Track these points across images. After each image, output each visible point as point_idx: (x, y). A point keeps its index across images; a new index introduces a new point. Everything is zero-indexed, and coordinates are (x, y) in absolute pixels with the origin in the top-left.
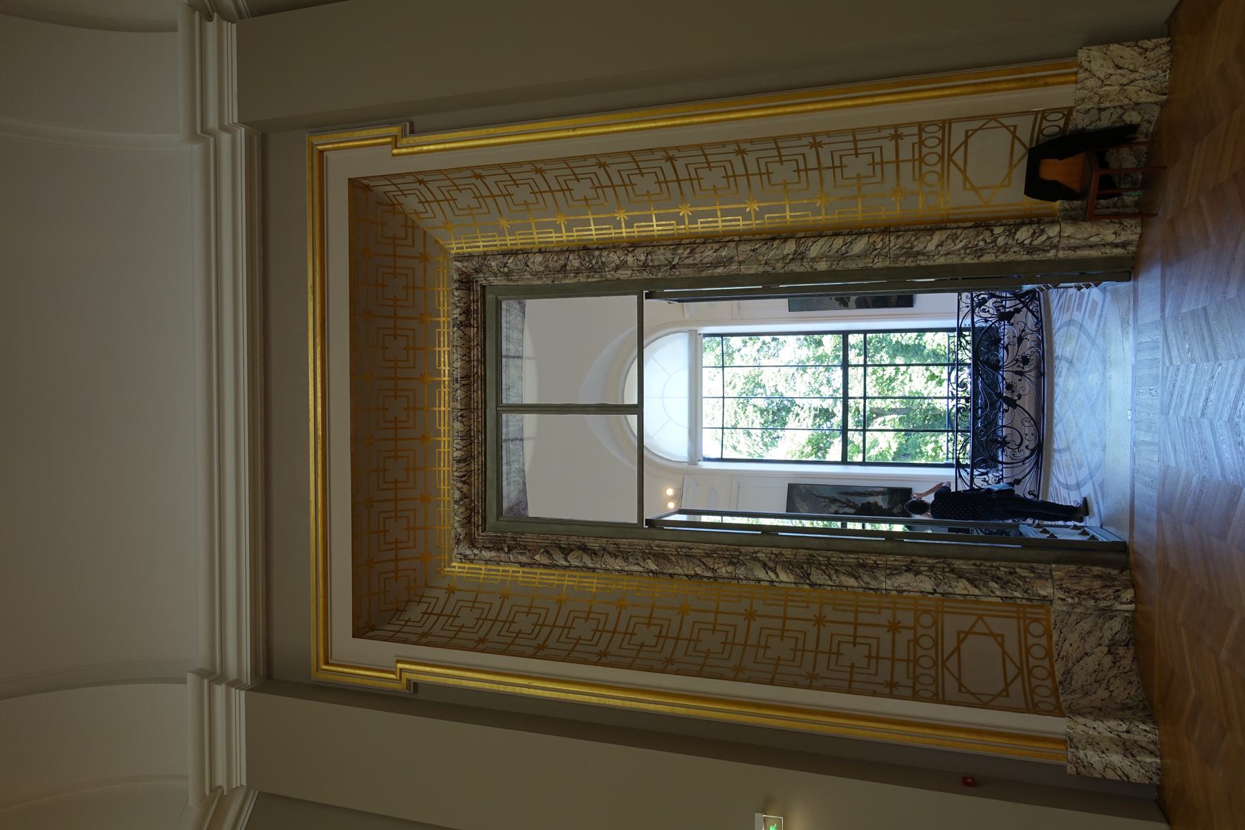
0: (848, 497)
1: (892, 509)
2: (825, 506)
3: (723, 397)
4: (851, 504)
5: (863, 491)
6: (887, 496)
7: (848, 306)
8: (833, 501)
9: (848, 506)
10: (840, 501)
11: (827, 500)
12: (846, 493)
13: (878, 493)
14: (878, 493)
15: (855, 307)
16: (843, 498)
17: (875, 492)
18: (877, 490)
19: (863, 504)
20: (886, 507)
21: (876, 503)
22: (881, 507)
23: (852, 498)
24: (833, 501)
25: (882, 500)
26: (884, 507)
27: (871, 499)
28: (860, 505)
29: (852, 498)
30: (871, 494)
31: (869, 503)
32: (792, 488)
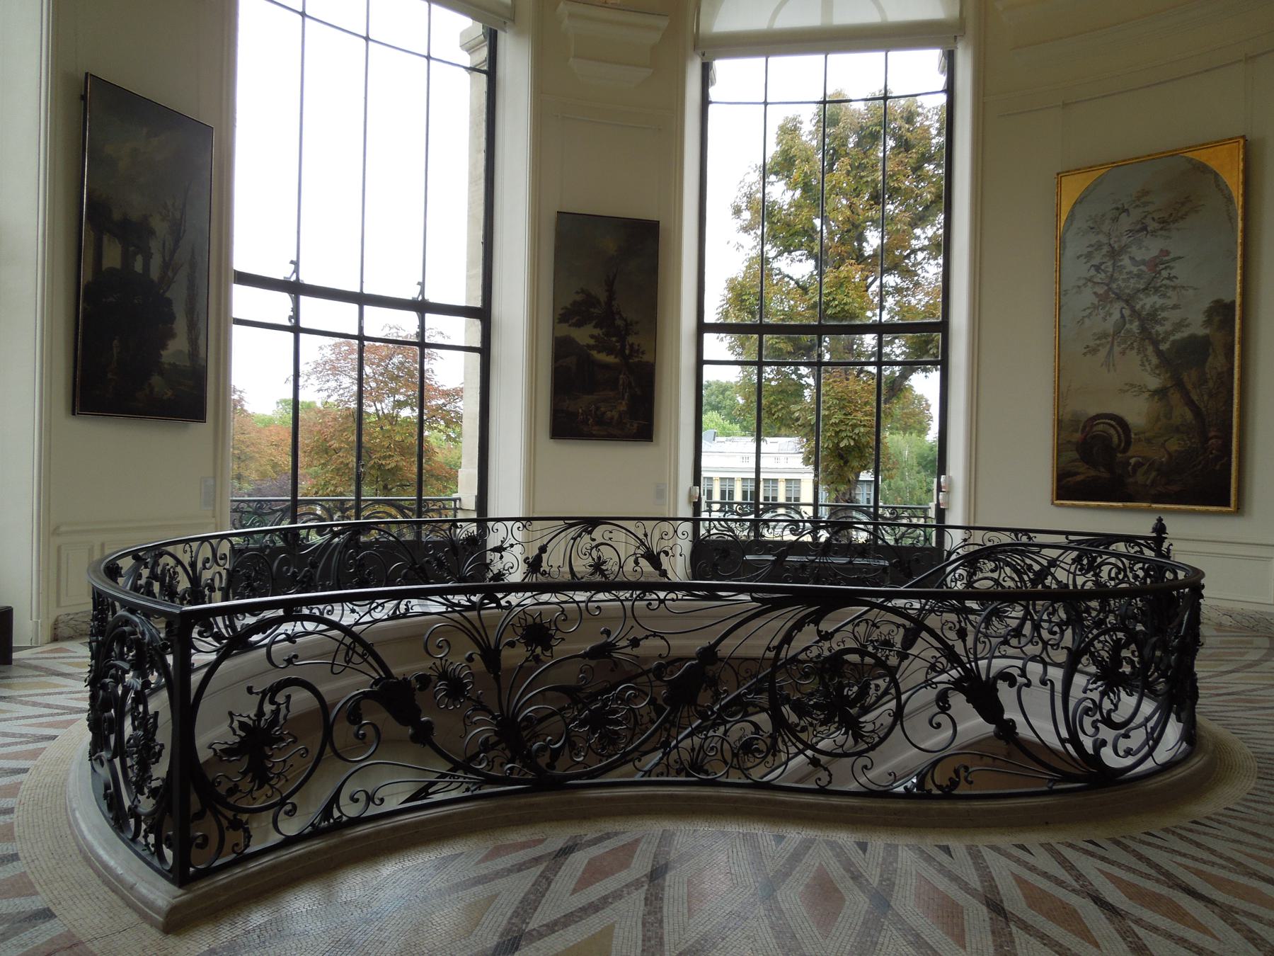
3: (766, 103)
9: (166, 266)
14: (194, 342)
15: (558, 334)
19: (169, 302)
20: (163, 360)
21: (171, 335)
22: (164, 346)
26: (164, 353)
27: (180, 325)
28: (168, 295)
30: (192, 326)
31: (171, 318)
32: (655, 225)
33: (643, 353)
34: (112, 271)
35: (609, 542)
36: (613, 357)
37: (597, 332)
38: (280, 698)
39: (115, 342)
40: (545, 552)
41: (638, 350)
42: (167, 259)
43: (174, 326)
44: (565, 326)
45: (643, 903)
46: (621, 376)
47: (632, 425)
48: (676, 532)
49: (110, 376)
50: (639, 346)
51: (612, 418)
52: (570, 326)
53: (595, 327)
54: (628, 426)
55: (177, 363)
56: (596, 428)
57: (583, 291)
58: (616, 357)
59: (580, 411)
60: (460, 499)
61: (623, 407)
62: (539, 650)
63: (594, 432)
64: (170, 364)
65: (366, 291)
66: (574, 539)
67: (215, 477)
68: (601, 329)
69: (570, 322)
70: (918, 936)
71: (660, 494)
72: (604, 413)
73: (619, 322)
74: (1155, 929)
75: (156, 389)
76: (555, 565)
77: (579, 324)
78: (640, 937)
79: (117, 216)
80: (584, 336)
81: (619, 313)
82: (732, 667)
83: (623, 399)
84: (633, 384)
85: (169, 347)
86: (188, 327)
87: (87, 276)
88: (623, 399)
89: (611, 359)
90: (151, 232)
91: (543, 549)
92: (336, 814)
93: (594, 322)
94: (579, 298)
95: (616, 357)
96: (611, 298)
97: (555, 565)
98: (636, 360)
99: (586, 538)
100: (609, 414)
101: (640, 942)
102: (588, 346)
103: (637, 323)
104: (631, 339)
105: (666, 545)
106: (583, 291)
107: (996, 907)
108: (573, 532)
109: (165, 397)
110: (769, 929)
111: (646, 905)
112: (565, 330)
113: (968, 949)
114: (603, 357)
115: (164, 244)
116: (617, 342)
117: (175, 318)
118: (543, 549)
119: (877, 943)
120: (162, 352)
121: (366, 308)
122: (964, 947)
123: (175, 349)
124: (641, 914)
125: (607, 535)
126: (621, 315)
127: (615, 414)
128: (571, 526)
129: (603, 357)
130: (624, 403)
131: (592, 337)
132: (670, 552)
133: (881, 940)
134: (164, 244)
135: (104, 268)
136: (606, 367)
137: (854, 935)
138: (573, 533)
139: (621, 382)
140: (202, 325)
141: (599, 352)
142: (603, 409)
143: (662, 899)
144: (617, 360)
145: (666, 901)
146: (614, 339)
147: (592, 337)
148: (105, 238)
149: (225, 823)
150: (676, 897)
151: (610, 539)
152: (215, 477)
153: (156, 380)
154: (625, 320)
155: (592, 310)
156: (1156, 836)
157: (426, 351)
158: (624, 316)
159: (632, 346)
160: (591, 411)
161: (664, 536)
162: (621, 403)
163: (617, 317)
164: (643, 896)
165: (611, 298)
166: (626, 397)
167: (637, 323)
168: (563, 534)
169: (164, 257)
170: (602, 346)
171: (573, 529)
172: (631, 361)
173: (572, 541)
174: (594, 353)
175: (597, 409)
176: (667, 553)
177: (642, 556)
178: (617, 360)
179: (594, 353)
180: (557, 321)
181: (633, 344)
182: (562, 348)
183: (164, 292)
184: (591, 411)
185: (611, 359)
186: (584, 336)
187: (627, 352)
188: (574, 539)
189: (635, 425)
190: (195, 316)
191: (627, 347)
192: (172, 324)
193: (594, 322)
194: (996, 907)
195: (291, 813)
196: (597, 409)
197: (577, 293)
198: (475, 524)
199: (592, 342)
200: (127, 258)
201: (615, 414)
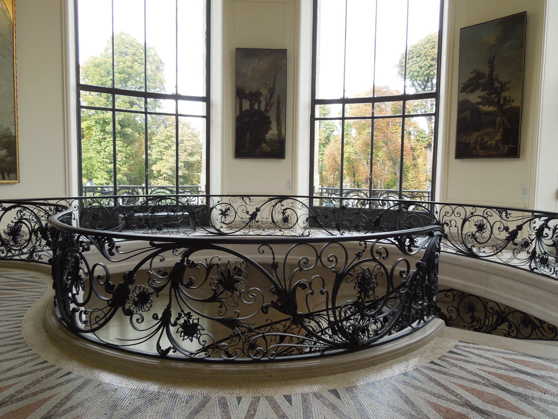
0: (276, 104)
1: (266, 143)
2: (266, 84)
4: (269, 107)
5: (281, 117)
6: (277, 138)
7: (461, 93)
8: (272, 92)
9: (267, 105)
10: (271, 97)
11: (272, 86)
12: (279, 103)
13: (279, 131)
14: (279, 131)
15: (460, 100)
16: (274, 100)
17: (281, 129)
18: (283, 130)
19: (269, 118)
20: (266, 138)
21: (270, 128)
22: (267, 133)
23: (274, 108)
24: (272, 92)
25: (274, 134)
27: (274, 125)
28: (268, 115)
29: (274, 108)
30: (279, 124)
31: (270, 123)
32: (283, 53)
33: (513, 101)
34: (246, 110)
36: (493, 107)
37: (483, 93)
39: (248, 134)
40: (259, 211)
41: (509, 100)
42: (267, 102)
43: (271, 125)
44: (464, 94)
46: (498, 118)
47: (504, 148)
48: (453, 212)
49: (246, 145)
50: (510, 97)
51: (491, 144)
52: (467, 93)
53: (482, 91)
54: (501, 149)
55: (272, 138)
56: (481, 151)
57: (475, 71)
59: (472, 142)
60: (200, 187)
61: (498, 137)
63: (480, 154)
64: (269, 139)
66: (274, 206)
68: (485, 91)
69: (467, 91)
71: (524, 191)
72: (487, 142)
73: (497, 85)
75: (264, 148)
76: (265, 217)
77: (472, 92)
79: (247, 92)
80: (474, 98)
81: (497, 79)
82: (482, 303)
83: (499, 132)
84: (506, 122)
85: (269, 133)
86: (277, 125)
87: (238, 114)
88: (499, 132)
89: (491, 109)
90: (261, 94)
91: (258, 210)
93: (481, 88)
94: (472, 76)
96: (492, 71)
97: (265, 217)
98: (508, 106)
100: (489, 143)
102: (478, 104)
103: (509, 83)
104: (504, 94)
105: (447, 219)
106: (475, 71)
108: (273, 202)
109: (268, 151)
112: (465, 96)
114: (486, 108)
115: (266, 97)
116: (495, 97)
117: (271, 123)
118: (258, 210)
120: (266, 135)
123: (272, 133)
126: (498, 80)
129: (486, 108)
130: (499, 134)
131: (480, 97)
132: (449, 223)
134: (266, 97)
135: (243, 110)
136: (488, 114)
138: (272, 203)
139: (497, 122)
140: (283, 123)
141: (484, 106)
142: (485, 140)
144: (495, 109)
146: (493, 96)
147: (480, 97)
148: (243, 100)
152: (292, 179)
153: (264, 145)
154: (501, 83)
155: (480, 81)
156: (37, 364)
157: (433, 117)
158: (500, 80)
159: (505, 98)
160: (478, 141)
161: (447, 214)
162: (497, 135)
163: (496, 82)
165: (492, 71)
167: (509, 83)
168: (269, 203)
170: (486, 101)
171: (272, 201)
172: (504, 108)
173: (272, 207)
175: (482, 140)
176: (447, 224)
178: (495, 109)
180: (460, 92)
181: (506, 97)
182: (463, 106)
183: (266, 115)
184: (478, 141)
185: (491, 109)
186: (474, 98)
187: (502, 102)
188: (274, 206)
190: (280, 121)
191: (502, 99)
192: (270, 125)
193: (481, 88)
196: (482, 140)
197: (471, 73)
198: (308, 198)
199: (479, 100)
200: (251, 105)
201: (493, 142)
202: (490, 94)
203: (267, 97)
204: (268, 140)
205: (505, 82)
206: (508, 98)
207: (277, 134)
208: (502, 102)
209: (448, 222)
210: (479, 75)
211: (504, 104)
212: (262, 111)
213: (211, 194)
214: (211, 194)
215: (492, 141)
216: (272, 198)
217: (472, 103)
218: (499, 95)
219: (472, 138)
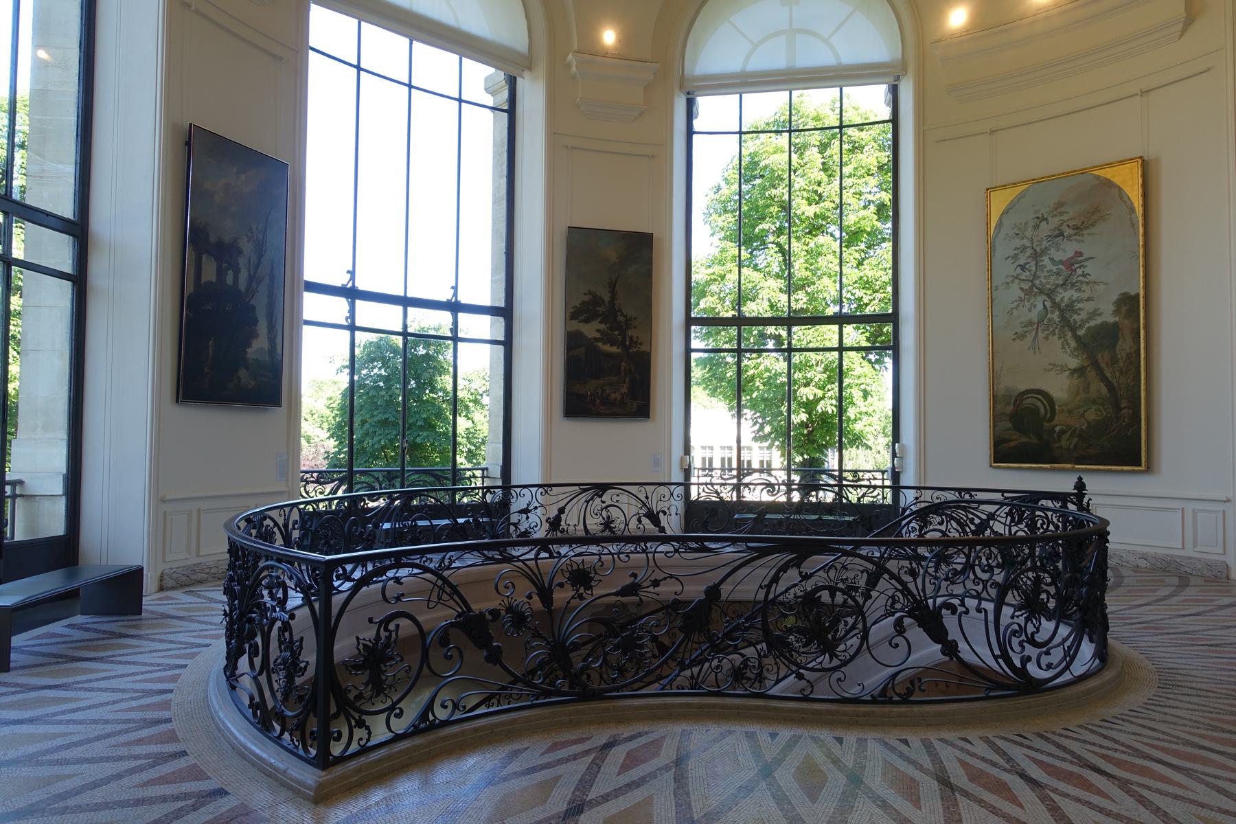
7: (571, 319)
9: (251, 279)
11: (261, 237)
12: (272, 278)
14: (272, 341)
15: (570, 329)
17: (275, 337)
19: (253, 307)
20: (248, 356)
21: (254, 335)
22: (249, 345)
26: (249, 350)
27: (262, 327)
28: (252, 302)
30: (271, 328)
31: (256, 321)
33: (641, 344)
35: (617, 504)
36: (615, 347)
37: (602, 327)
38: (392, 626)
39: (211, 342)
40: (564, 513)
41: (637, 342)
45: (672, 781)
47: (632, 405)
48: (672, 494)
51: (616, 399)
53: (600, 323)
54: (629, 405)
55: (260, 359)
56: (601, 408)
58: (618, 348)
61: (624, 390)
62: (582, 590)
64: (253, 359)
65: (409, 295)
66: (588, 502)
67: (288, 453)
70: (884, 801)
71: (656, 462)
72: (609, 395)
73: (621, 318)
74: (1067, 796)
75: (242, 381)
77: (587, 321)
78: (674, 804)
79: (213, 239)
80: (591, 330)
81: (620, 311)
83: (625, 383)
84: (633, 370)
85: (253, 345)
86: (268, 328)
88: (625, 383)
89: (614, 349)
90: (240, 252)
91: (562, 511)
92: (431, 718)
94: (587, 298)
95: (618, 348)
98: (635, 350)
99: (598, 500)
100: (613, 396)
101: (674, 808)
102: (596, 340)
104: (630, 333)
105: (661, 506)
106: (590, 293)
107: (944, 781)
109: (250, 387)
110: (771, 798)
111: (675, 782)
112: (576, 325)
113: (923, 810)
114: (607, 348)
117: (257, 321)
118: (562, 511)
119: (853, 807)
121: (410, 309)
122: (921, 809)
123: (259, 344)
124: (672, 788)
125: (615, 498)
127: (617, 396)
128: (585, 490)
129: (607, 348)
131: (598, 331)
132: (667, 511)
133: (856, 804)
135: (203, 282)
136: (610, 356)
137: (836, 801)
139: (623, 369)
141: (604, 344)
142: (607, 392)
143: (687, 778)
144: (619, 350)
145: (690, 780)
146: (616, 333)
147: (598, 331)
148: (204, 257)
149: (353, 723)
150: (698, 776)
151: (617, 501)
152: (288, 453)
153: (243, 373)
154: (626, 316)
155: (598, 308)
158: (625, 313)
159: (631, 338)
163: (619, 314)
164: (672, 776)
166: (627, 380)
167: (635, 319)
169: (249, 271)
174: (600, 344)
175: (603, 391)
176: (665, 513)
177: (644, 515)
178: (619, 350)
179: (600, 344)
182: (573, 341)
185: (614, 349)
186: (591, 330)
187: (628, 343)
188: (588, 502)
189: (635, 405)
192: (256, 326)
193: (599, 319)
194: (944, 781)
195: (399, 716)
199: (598, 335)
200: (221, 273)
202: (611, 329)
203: (252, 261)
204: (251, 361)
205: (631, 317)
206: (635, 339)
207: (267, 349)
208: (628, 343)
209: (666, 509)
210: (596, 300)
211: (630, 346)
212: (240, 291)
213: (514, 483)
214: (514, 483)
215: (617, 395)
216: (586, 487)
217: (586, 337)
218: (623, 333)
219: (590, 387)
